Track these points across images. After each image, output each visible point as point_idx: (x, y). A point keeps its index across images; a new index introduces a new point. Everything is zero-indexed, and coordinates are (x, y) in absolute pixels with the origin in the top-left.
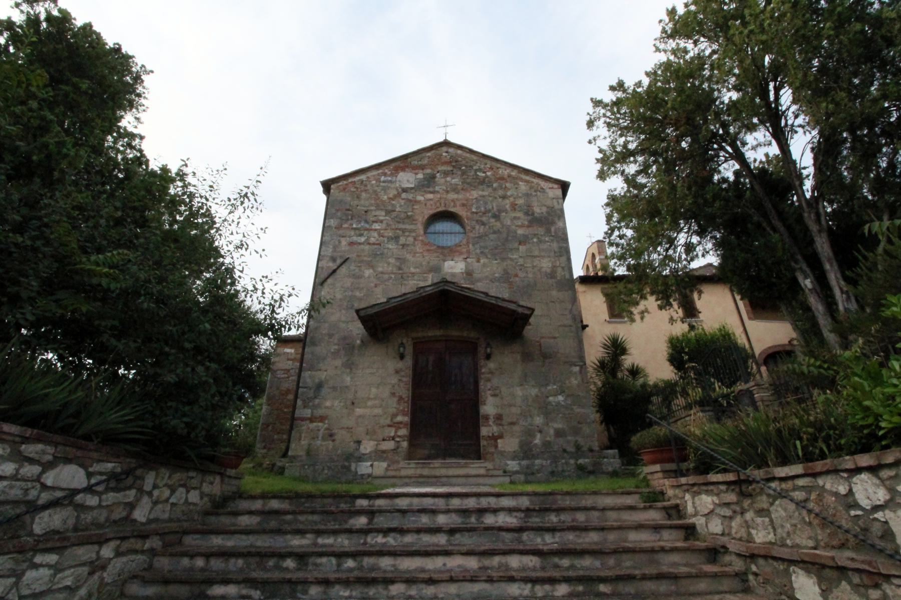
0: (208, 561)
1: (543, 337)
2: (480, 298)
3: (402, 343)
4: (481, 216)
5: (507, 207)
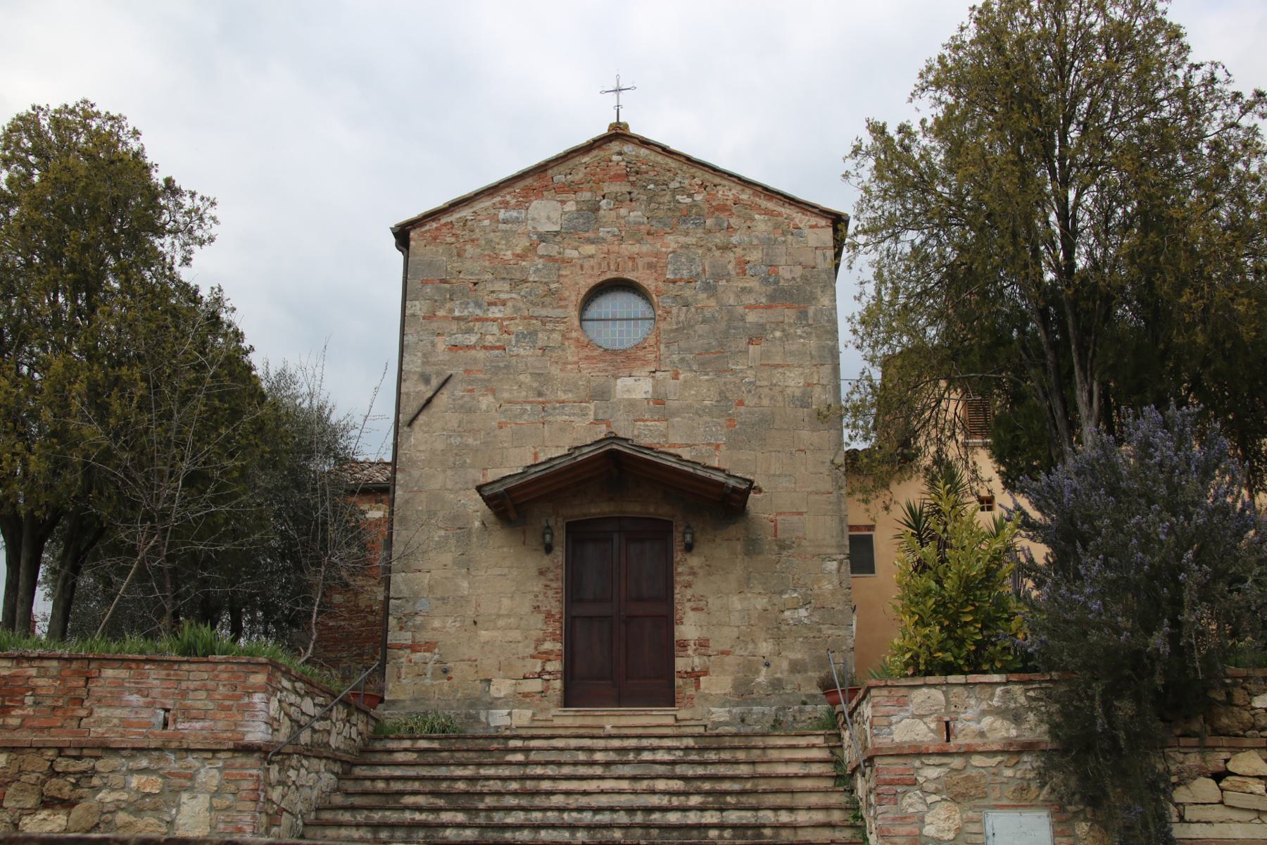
0: (388, 784)
1: (781, 514)
2: (669, 464)
3: (548, 527)
4: (682, 288)
5: (730, 267)
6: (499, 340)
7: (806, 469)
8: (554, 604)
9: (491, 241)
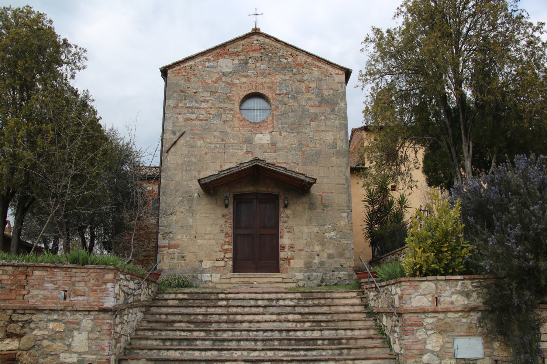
0: (167, 316)
2: (281, 171)
3: (227, 197)
5: (303, 89)
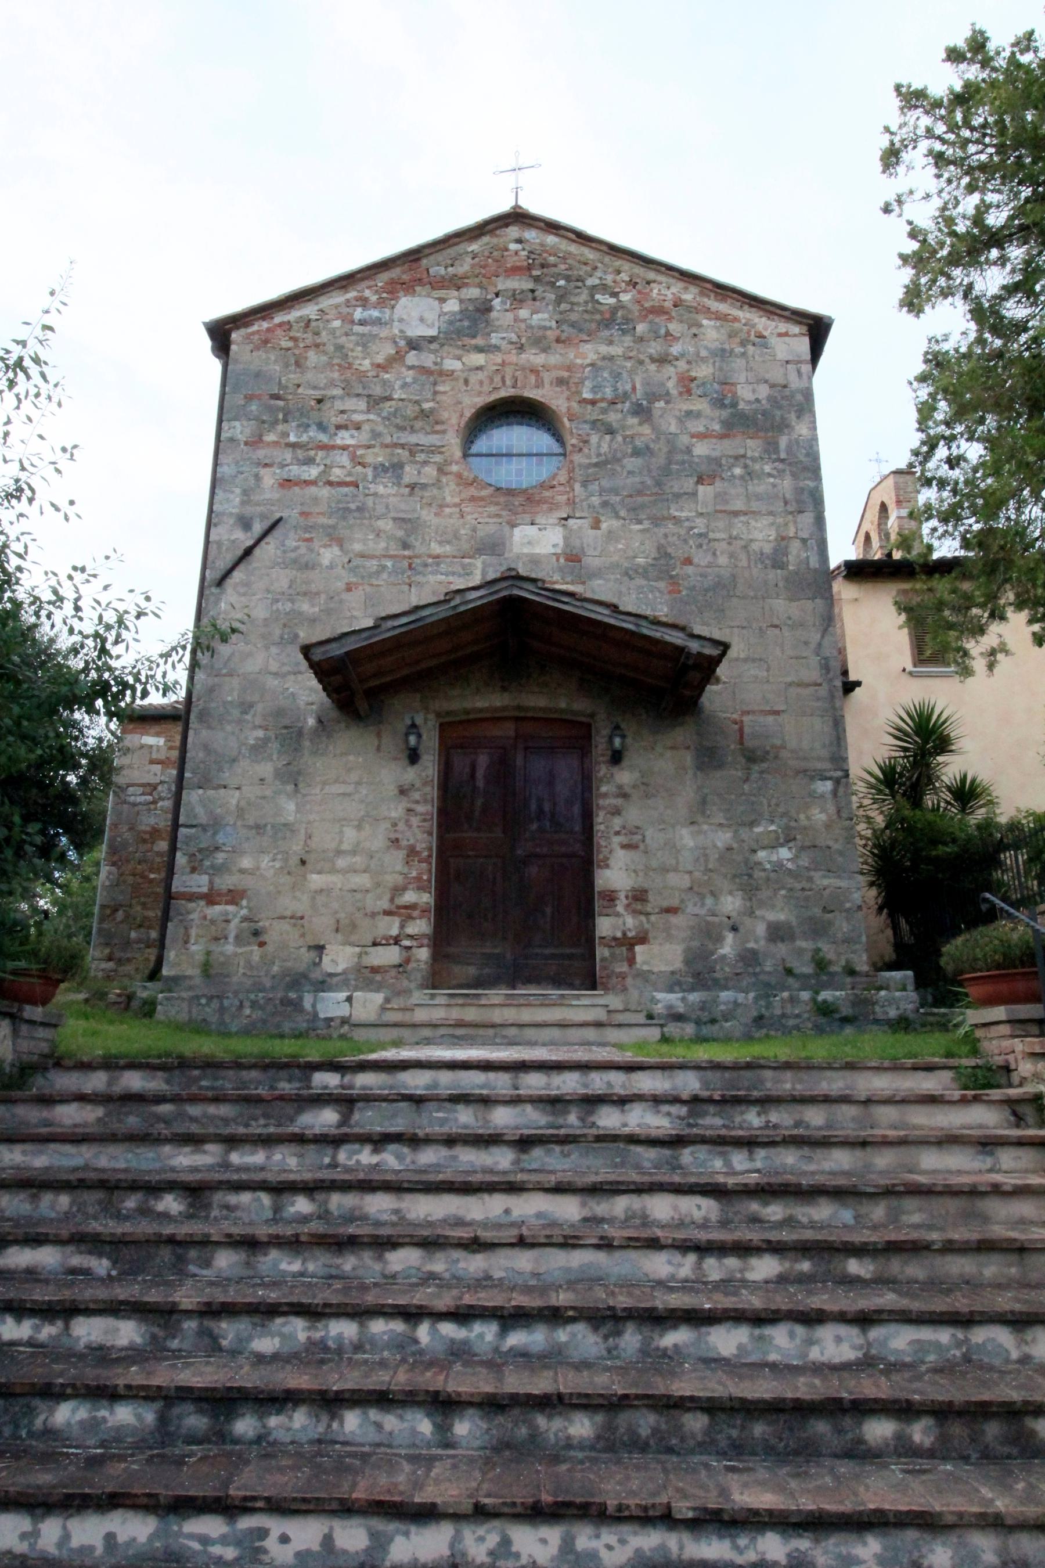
1: (748, 713)
2: (599, 618)
3: (414, 725)
4: (604, 411)
5: (670, 384)
6: (350, 474)
7: (783, 652)
8: (420, 836)
9: (343, 347)
